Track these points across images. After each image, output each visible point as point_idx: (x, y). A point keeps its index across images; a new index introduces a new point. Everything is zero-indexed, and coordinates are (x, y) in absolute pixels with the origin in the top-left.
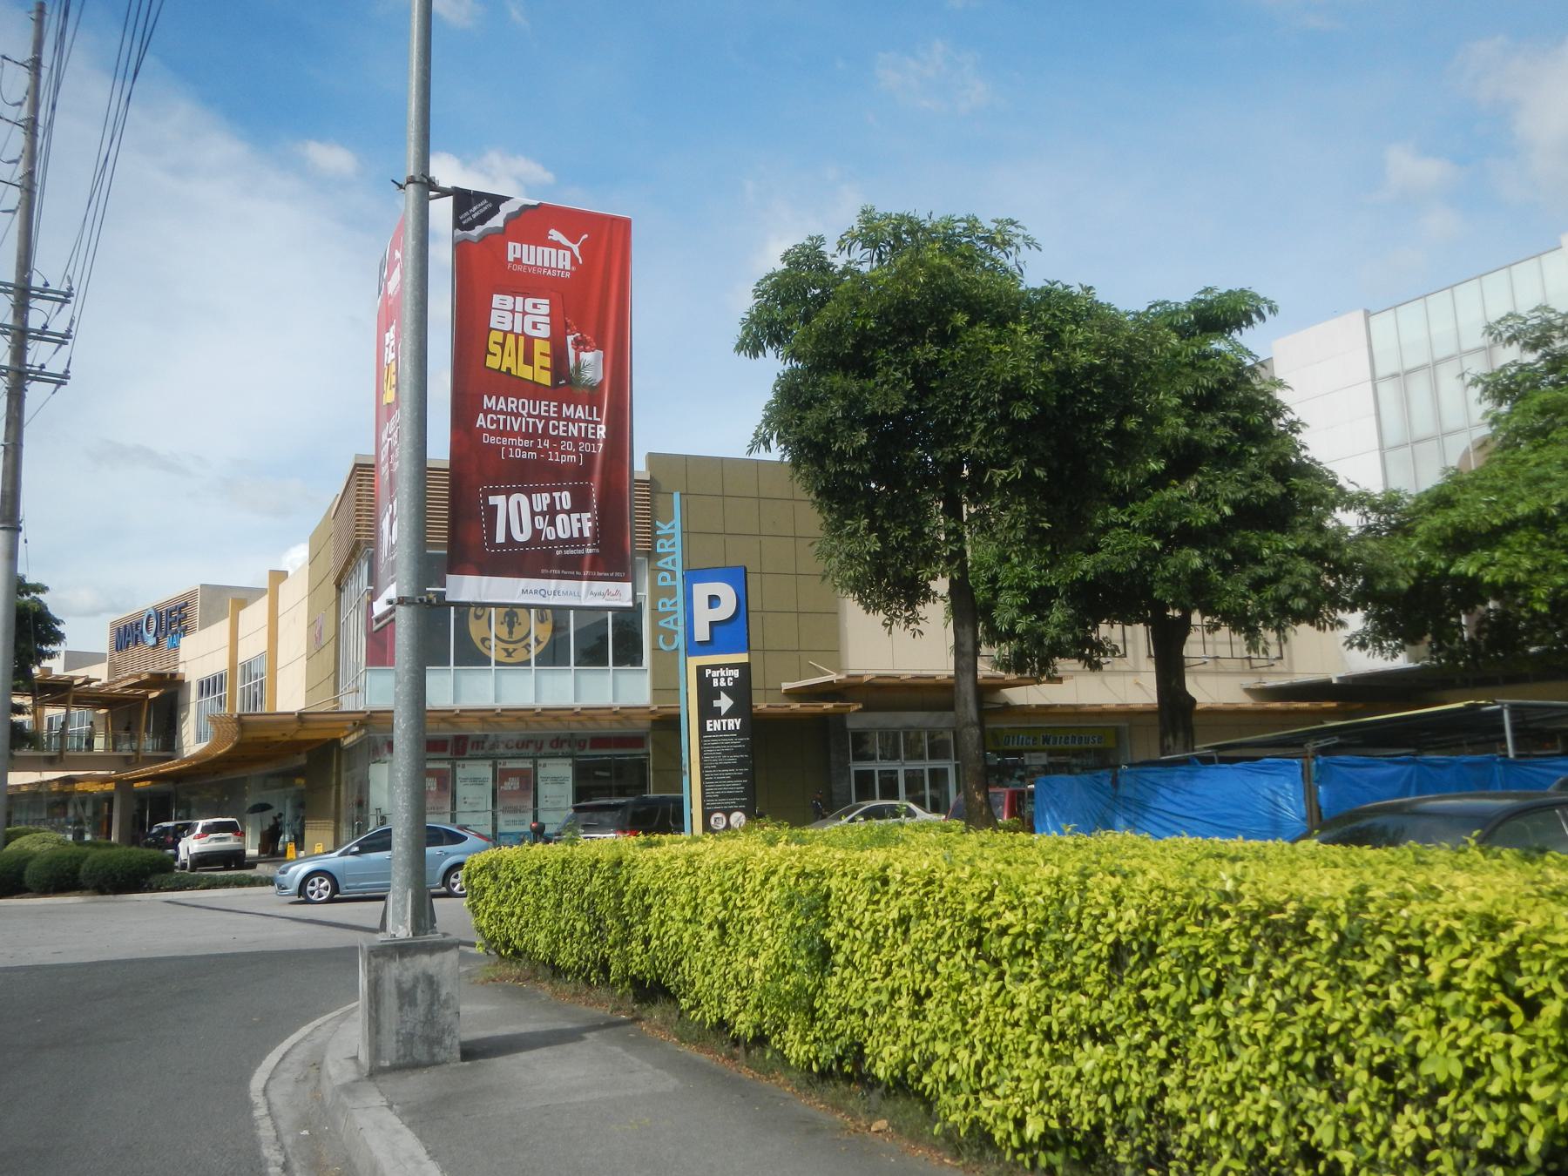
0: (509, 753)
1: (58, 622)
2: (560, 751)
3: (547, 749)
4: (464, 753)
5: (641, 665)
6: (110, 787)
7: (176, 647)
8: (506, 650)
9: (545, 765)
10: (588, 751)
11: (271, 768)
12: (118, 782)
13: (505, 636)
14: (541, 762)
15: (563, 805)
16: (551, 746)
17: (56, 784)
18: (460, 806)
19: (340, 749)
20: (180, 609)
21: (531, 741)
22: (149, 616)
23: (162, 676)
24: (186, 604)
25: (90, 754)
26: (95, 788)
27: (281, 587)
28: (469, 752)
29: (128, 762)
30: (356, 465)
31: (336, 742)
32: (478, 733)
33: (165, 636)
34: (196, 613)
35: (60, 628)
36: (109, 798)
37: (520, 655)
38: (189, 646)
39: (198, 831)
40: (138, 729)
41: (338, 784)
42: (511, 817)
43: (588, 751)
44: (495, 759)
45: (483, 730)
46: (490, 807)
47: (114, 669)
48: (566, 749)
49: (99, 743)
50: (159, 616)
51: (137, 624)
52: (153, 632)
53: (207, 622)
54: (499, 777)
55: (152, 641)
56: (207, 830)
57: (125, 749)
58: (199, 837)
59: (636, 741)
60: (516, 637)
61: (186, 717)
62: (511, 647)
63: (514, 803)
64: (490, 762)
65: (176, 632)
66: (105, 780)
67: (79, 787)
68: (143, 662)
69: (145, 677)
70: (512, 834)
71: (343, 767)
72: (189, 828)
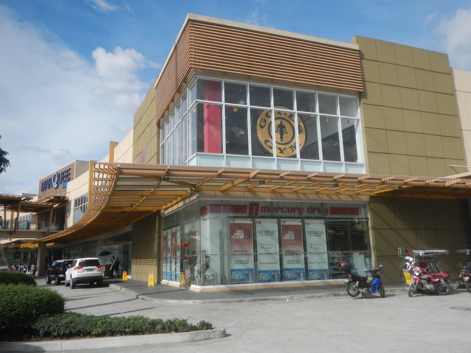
0: (284, 215)
1: (5, 153)
2: (313, 215)
3: (305, 214)
4: (257, 214)
5: (356, 162)
6: (37, 245)
7: (65, 187)
8: (280, 149)
9: (309, 224)
10: (329, 216)
11: (108, 235)
12: (39, 242)
13: (279, 141)
14: (306, 221)
15: (321, 250)
16: (308, 212)
17: (13, 244)
18: (259, 250)
19: (160, 217)
20: (67, 171)
21: (297, 208)
22: (55, 176)
23: (59, 197)
24: (70, 169)
25: (28, 230)
26: (31, 246)
27: (115, 149)
28: (260, 214)
29: (44, 234)
30: (189, 20)
31: (158, 212)
32: (268, 200)
33: (61, 182)
34: (74, 172)
35: (6, 157)
36: (36, 250)
37: (288, 151)
38: (70, 185)
39: (77, 265)
40: (49, 220)
41: (159, 238)
42: (290, 258)
43: (329, 216)
44: (278, 218)
45: (272, 198)
46: (278, 251)
47: (40, 197)
48: (316, 214)
49: (33, 227)
50: (59, 175)
51: (50, 180)
52: (56, 182)
53: (78, 175)
54: (282, 230)
55: (55, 186)
56: (82, 265)
57: (44, 230)
58: (78, 268)
59: (354, 210)
60: (285, 140)
61: (69, 215)
62: (282, 147)
63: (292, 248)
64: (276, 220)
65: (66, 181)
66: (34, 242)
67: (22, 246)
68: (51, 193)
69: (52, 198)
70: (292, 270)
71: (162, 228)
72: (72, 264)
